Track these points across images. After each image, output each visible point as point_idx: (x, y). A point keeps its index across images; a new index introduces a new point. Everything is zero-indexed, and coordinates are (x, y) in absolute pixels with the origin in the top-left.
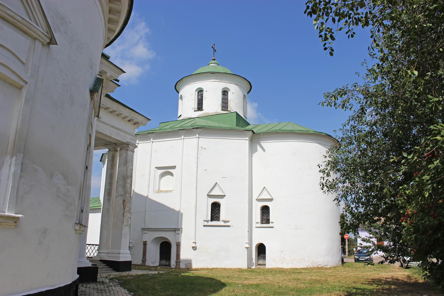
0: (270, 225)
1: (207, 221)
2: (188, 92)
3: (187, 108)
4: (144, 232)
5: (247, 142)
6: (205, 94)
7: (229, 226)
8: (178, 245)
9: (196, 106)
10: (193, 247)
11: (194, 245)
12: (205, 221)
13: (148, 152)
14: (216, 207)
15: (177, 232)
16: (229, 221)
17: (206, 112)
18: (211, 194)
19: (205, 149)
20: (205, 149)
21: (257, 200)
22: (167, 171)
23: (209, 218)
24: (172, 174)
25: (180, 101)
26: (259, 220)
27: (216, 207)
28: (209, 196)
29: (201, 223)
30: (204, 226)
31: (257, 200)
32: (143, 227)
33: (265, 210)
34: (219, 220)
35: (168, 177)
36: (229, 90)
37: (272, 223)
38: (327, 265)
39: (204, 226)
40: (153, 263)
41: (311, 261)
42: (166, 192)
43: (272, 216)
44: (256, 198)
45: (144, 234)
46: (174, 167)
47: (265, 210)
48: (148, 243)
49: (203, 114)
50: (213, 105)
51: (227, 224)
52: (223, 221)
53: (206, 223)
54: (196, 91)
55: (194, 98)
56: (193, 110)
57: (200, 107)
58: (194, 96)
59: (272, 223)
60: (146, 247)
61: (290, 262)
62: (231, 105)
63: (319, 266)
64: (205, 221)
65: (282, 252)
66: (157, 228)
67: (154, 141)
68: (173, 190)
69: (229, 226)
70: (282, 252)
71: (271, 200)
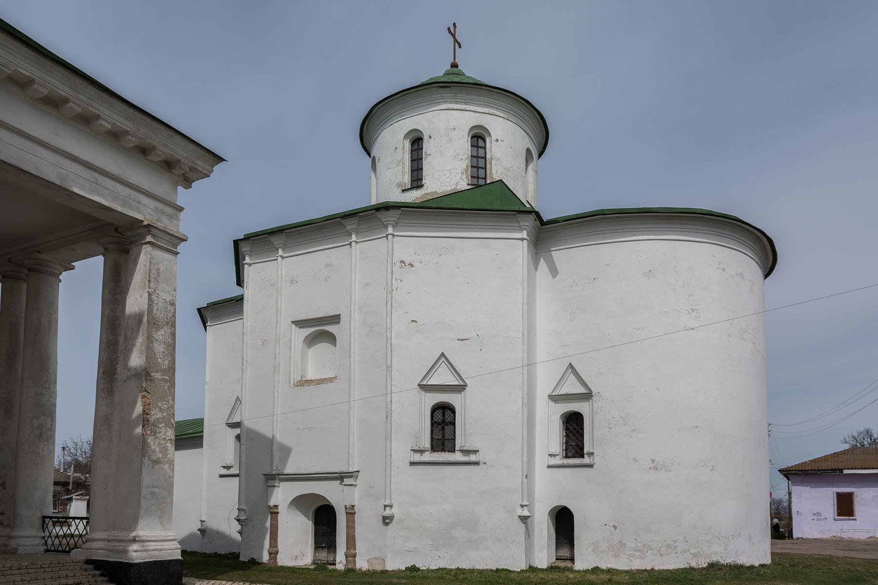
0: (586, 460)
1: (422, 452)
4: (270, 483)
6: (428, 146)
7: (476, 463)
8: (351, 512)
9: (407, 179)
10: (385, 518)
12: (415, 451)
15: (347, 481)
16: (475, 452)
17: (429, 191)
18: (433, 382)
21: (551, 397)
22: (321, 330)
23: (427, 444)
24: (331, 338)
28: (425, 388)
30: (412, 464)
31: (551, 397)
32: (268, 471)
33: (573, 424)
34: (453, 450)
35: (323, 347)
39: (412, 464)
40: (296, 558)
42: (320, 382)
43: (593, 436)
44: (549, 392)
45: (270, 489)
47: (573, 424)
48: (280, 510)
51: (473, 458)
53: (417, 457)
56: (400, 190)
59: (591, 454)
60: (277, 520)
62: (494, 171)
64: (415, 451)
66: (302, 472)
67: (285, 255)
68: (335, 378)
69: (476, 463)
70: (615, 528)
71: (587, 396)
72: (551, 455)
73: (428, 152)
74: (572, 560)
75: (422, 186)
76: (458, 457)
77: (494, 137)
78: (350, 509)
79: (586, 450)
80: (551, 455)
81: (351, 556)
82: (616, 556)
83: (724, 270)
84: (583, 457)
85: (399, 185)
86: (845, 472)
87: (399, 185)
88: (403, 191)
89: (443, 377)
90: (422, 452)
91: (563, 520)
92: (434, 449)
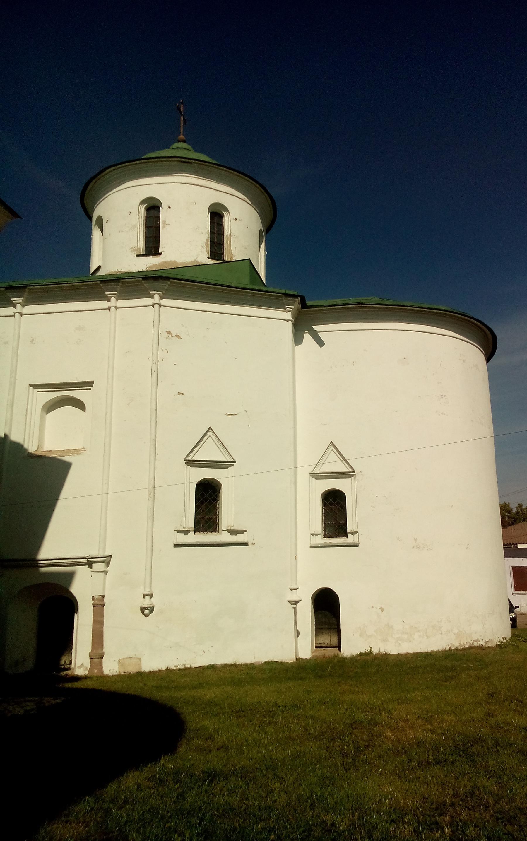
0: (350, 539)
1: (186, 532)
2: (120, 207)
3: (115, 246)
5: (289, 326)
6: (164, 215)
8: (99, 605)
9: (141, 245)
10: (143, 610)
11: (147, 603)
12: (179, 532)
13: (6, 343)
14: (208, 495)
16: (242, 532)
17: (168, 259)
18: (198, 457)
19: (178, 336)
20: (178, 336)
23: (191, 524)
25: (96, 233)
26: (318, 527)
27: (208, 495)
28: (192, 463)
29: (167, 536)
30: (176, 546)
36: (226, 210)
37: (353, 533)
38: (491, 641)
41: (456, 631)
44: (310, 469)
46: (89, 384)
49: (160, 265)
50: (184, 244)
51: (239, 538)
52: (228, 531)
53: (182, 539)
54: (143, 202)
55: (134, 222)
56: (134, 254)
57: (152, 246)
58: (134, 215)
59: (353, 533)
61: (405, 637)
63: (475, 644)
64: (179, 532)
65: (382, 609)
68: (83, 449)
70: (382, 609)
71: (349, 474)
72: (313, 535)
73: (167, 222)
74: (339, 647)
75: (161, 254)
76: (224, 537)
77: (233, 216)
78: (98, 599)
79: (349, 530)
80: (313, 535)
81: (97, 656)
82: (385, 640)
83: (464, 361)
84: (344, 534)
85: (133, 249)
86: (520, 546)
87: (133, 249)
88: (138, 256)
89: (209, 452)
90: (186, 532)
91: (326, 605)
92: (197, 529)
